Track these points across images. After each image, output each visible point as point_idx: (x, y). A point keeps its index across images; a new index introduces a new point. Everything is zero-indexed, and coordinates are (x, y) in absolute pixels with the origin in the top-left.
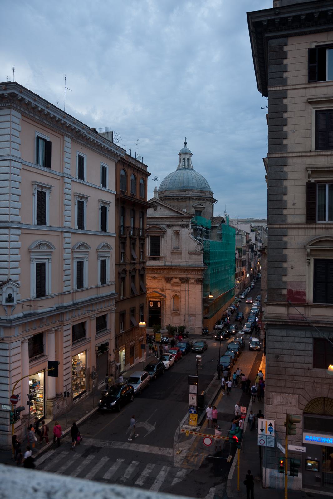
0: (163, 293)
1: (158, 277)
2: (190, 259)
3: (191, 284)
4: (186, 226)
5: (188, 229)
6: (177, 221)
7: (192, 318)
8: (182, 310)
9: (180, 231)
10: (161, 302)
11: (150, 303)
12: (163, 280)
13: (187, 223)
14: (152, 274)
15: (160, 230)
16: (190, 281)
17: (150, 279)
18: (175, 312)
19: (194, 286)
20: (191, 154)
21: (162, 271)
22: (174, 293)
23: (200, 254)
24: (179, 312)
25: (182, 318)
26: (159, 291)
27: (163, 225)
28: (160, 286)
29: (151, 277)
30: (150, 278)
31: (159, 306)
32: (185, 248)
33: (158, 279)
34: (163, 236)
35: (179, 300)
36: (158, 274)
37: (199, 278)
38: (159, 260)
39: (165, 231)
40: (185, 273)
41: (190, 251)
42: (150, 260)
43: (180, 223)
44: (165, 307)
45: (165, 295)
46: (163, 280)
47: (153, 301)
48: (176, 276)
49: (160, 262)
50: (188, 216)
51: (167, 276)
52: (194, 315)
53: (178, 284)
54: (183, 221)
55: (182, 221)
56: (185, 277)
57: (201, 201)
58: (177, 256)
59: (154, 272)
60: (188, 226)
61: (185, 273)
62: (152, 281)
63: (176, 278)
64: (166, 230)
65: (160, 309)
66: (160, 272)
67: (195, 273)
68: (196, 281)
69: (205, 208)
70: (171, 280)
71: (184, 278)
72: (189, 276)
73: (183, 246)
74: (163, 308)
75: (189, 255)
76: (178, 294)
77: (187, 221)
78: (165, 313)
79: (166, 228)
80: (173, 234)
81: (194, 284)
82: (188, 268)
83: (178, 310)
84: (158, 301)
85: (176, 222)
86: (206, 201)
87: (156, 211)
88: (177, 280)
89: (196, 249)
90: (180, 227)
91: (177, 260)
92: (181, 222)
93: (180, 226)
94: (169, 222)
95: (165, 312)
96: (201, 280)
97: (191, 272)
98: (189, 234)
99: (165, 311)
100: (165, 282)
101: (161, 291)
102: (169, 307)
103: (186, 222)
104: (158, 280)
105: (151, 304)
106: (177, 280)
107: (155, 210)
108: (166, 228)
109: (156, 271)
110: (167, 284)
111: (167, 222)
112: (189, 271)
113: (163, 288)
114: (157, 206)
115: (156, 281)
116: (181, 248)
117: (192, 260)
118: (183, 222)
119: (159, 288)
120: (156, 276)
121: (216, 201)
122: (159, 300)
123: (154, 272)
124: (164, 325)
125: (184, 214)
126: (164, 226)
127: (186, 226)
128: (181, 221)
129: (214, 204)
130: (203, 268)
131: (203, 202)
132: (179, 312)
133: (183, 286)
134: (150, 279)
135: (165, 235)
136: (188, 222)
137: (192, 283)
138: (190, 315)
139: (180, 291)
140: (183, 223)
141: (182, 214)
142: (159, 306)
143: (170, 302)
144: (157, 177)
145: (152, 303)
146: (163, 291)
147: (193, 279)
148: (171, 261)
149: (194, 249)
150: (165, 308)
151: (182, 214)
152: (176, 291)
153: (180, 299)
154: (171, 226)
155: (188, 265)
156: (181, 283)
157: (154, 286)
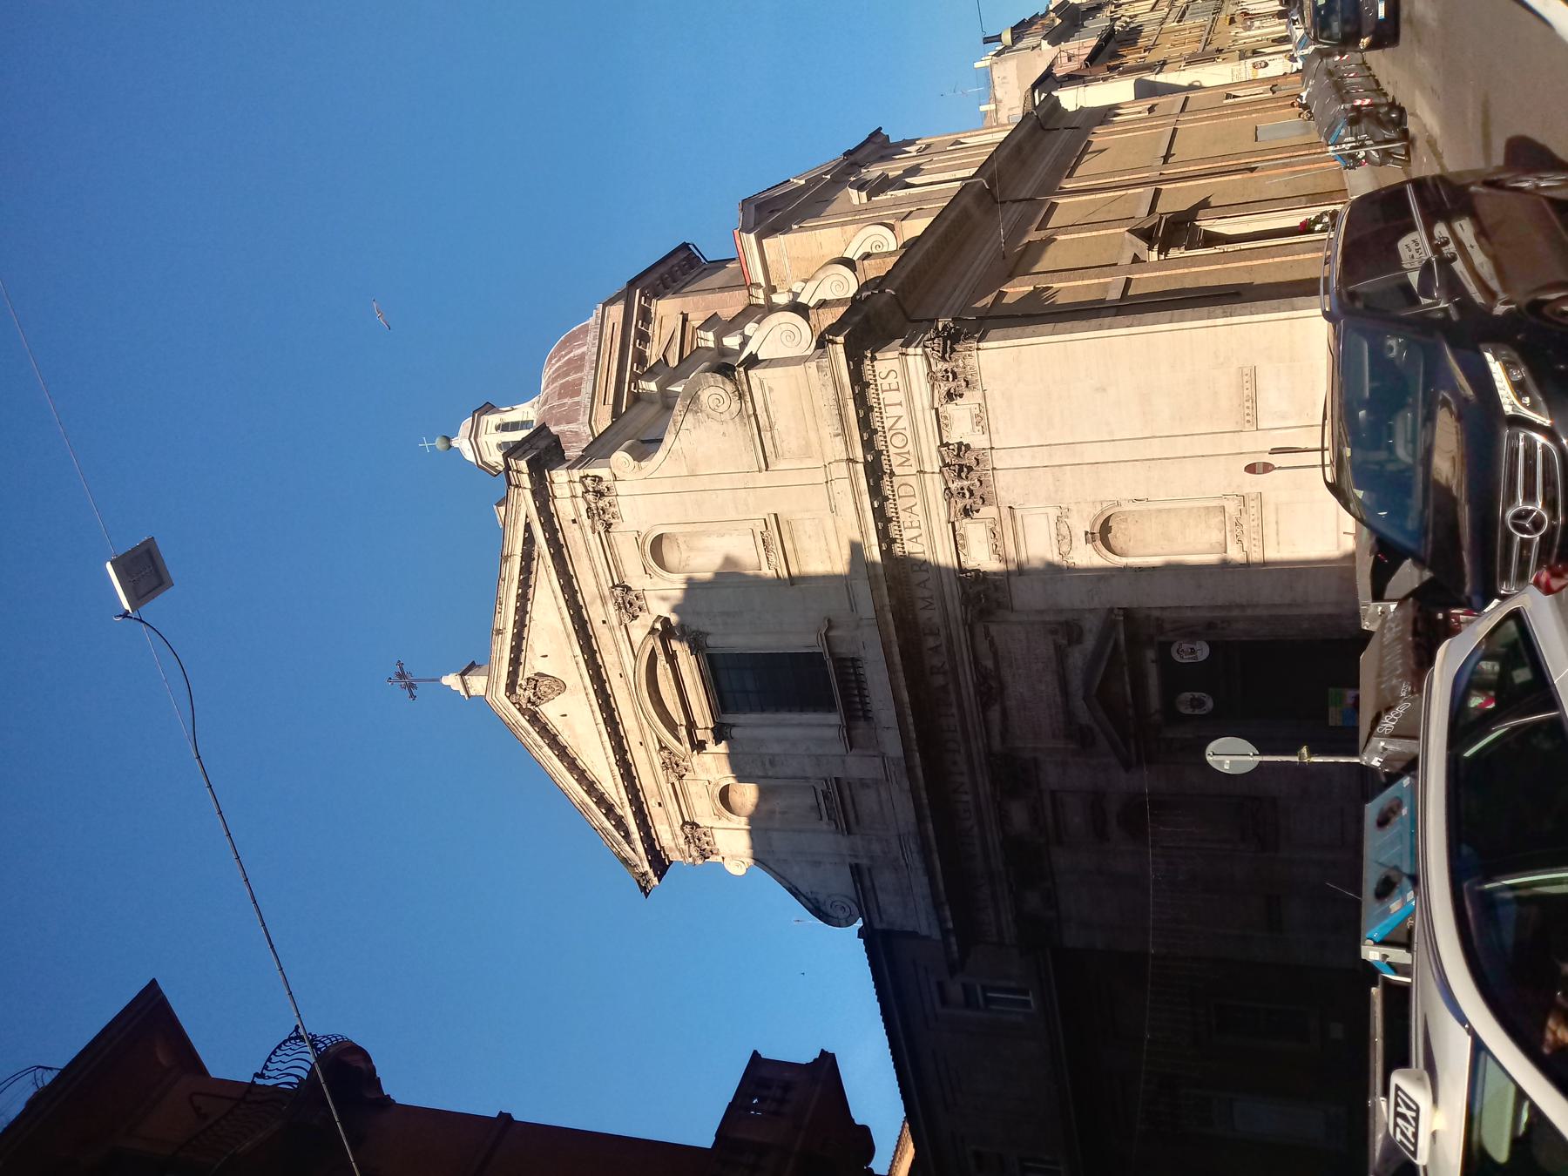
3: (987, 430)
9: (643, 531)
10: (1162, 638)
12: (993, 629)
14: (960, 706)
19: (996, 404)
24: (1232, 507)
29: (985, 707)
33: (989, 664)
43: (594, 541)
50: (528, 494)
52: (1250, 378)
53: (1007, 522)
55: (574, 521)
56: (938, 477)
59: (944, 688)
61: (913, 481)
64: (659, 617)
66: (936, 649)
75: (782, 465)
78: (1249, 612)
82: (860, 467)
90: (616, 535)
92: (581, 528)
95: (1242, 607)
99: (1235, 613)
105: (1199, 703)
107: (559, 686)
109: (939, 680)
110: (1017, 603)
113: (1054, 632)
122: (1151, 654)
126: (639, 631)
127: (599, 494)
128: (576, 526)
132: (1232, 507)
133: (1006, 486)
134: (1004, 713)
137: (981, 420)
140: (587, 522)
141: (528, 527)
142: (1203, 652)
144: (394, 677)
145: (1187, 695)
149: (731, 427)
151: (528, 527)
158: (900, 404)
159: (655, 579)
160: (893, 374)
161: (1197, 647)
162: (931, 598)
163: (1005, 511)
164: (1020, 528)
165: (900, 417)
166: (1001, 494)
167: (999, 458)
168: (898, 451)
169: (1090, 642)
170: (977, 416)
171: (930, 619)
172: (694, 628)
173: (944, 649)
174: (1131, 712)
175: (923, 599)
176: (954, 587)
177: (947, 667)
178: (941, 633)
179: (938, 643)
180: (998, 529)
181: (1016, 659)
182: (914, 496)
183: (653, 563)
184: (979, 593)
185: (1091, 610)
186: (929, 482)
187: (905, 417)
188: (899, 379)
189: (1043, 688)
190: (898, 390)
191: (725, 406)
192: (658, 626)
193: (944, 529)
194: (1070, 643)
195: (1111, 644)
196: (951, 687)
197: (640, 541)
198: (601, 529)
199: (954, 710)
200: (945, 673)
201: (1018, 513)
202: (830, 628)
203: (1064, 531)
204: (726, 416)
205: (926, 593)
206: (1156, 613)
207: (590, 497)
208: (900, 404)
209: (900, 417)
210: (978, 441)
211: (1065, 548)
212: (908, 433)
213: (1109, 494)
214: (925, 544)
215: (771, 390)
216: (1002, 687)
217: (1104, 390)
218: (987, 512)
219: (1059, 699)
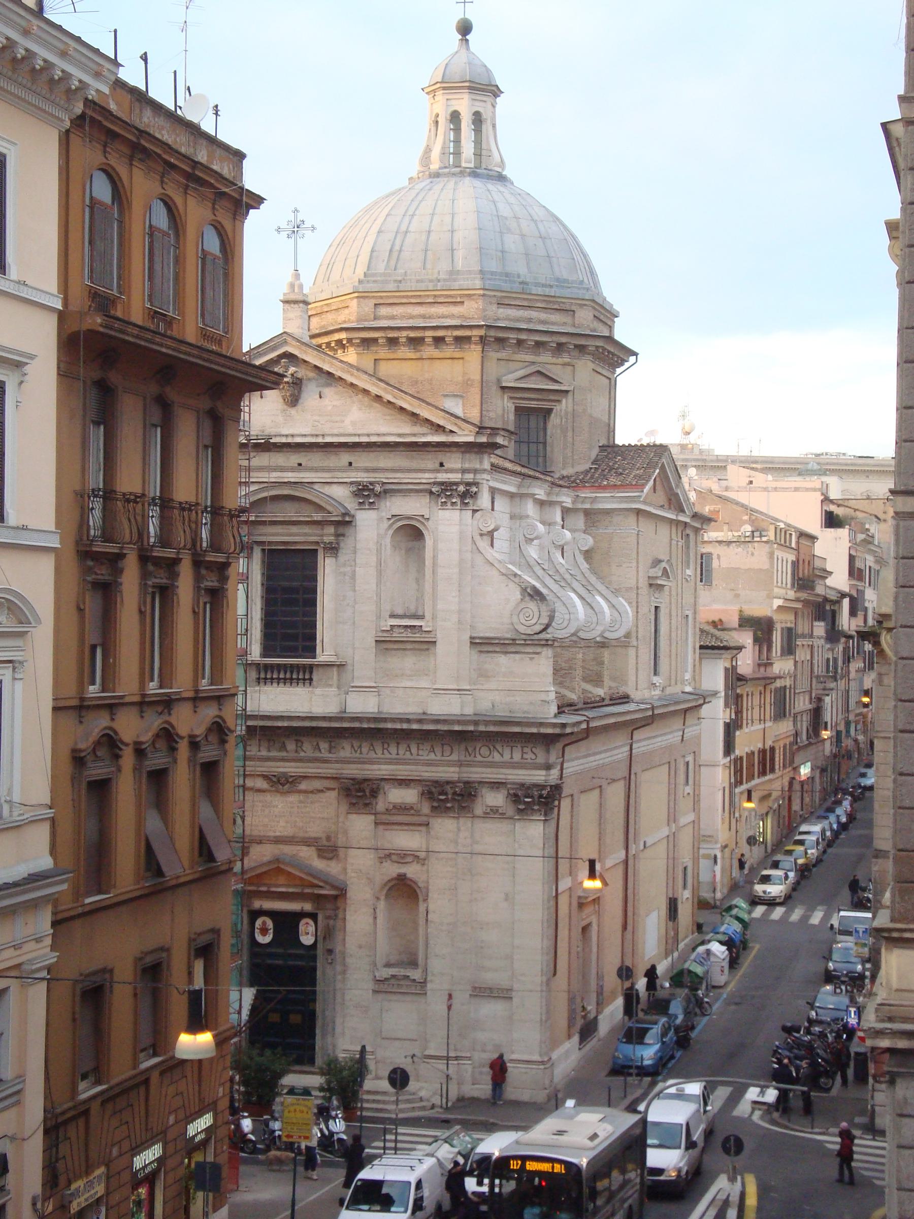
0: (332, 868)
1: (305, 777)
2: (483, 675)
4: (463, 496)
5: (475, 511)
6: (414, 464)
7: (490, 1009)
8: (435, 965)
10: (320, 918)
11: (259, 923)
12: (334, 794)
13: (469, 477)
14: (268, 759)
15: (318, 517)
16: (480, 799)
17: (259, 791)
18: (393, 976)
19: (505, 826)
20: (495, 92)
21: (324, 746)
22: (392, 870)
23: (539, 649)
24: (416, 974)
25: (436, 1004)
26: (307, 854)
27: (334, 487)
28: (315, 830)
29: (265, 777)
30: (261, 783)
31: (307, 940)
32: (455, 618)
33: (303, 786)
34: (333, 549)
35: (422, 907)
36: (301, 760)
37: (536, 785)
38: (311, 679)
39: (345, 523)
40: (454, 757)
41: (485, 630)
42: (258, 680)
44: (338, 948)
45: (341, 877)
46: (334, 794)
47: (271, 914)
48: (403, 771)
49: (318, 691)
50: (471, 439)
51: (353, 771)
52: (504, 994)
54: (447, 465)
55: (442, 465)
56: (455, 777)
57: (546, 358)
58: (408, 661)
60: (474, 496)
62: (268, 797)
63: (404, 783)
64: (353, 516)
65: (314, 958)
67: (507, 757)
68: (515, 798)
69: (570, 394)
70: (374, 793)
71: (448, 783)
72: (476, 774)
73: (440, 606)
74: (330, 951)
75: (475, 655)
76: (412, 871)
77: (467, 466)
79: (351, 505)
80: (388, 540)
81: (503, 816)
83: (414, 964)
84: (302, 915)
85: (409, 471)
86: (576, 353)
87: (293, 411)
88: (409, 796)
89: (515, 619)
90: (426, 499)
91: (409, 684)
92: (438, 471)
93: (431, 493)
94: (367, 470)
96: (541, 796)
97: (485, 751)
98: (477, 538)
100: (344, 807)
101: (320, 856)
102: (360, 947)
103: (464, 471)
104: (305, 792)
105: (264, 931)
106: (409, 796)
107: (293, 401)
108: (351, 505)
110: (353, 817)
111: (358, 469)
112: (478, 745)
113: (328, 838)
114: (297, 383)
115: (293, 798)
116: (434, 618)
117: (493, 685)
118: (447, 471)
119: (307, 842)
120: (291, 769)
121: (632, 359)
122: (308, 907)
123: (283, 748)
124: (334, 1046)
125: (449, 427)
126: (340, 493)
127: (463, 496)
128: (437, 465)
129: (618, 371)
130: (554, 725)
131: (560, 361)
132: (416, 974)
134: (259, 791)
135: (346, 545)
136: (475, 471)
137: (493, 813)
138: (482, 992)
139: (422, 855)
140: (442, 477)
142: (307, 940)
143: (371, 920)
144: (300, 217)
145: (270, 924)
146: (331, 859)
147: (496, 785)
148: (376, 689)
150: (343, 953)
151: (440, 428)
152: (402, 857)
153: (425, 900)
154: (378, 495)
155: (469, 710)
156: (434, 809)
157: (281, 828)
158: (512, 758)
159: (386, 524)
160: (534, 757)
161: (309, 936)
162: (361, 753)
163: (424, 819)
164: (411, 828)
165: (502, 756)
166: (439, 820)
167: (465, 823)
168: (477, 749)
169: (319, 864)
170: (497, 811)
171: (343, 748)
172: (342, 545)
173: (318, 755)
174: (264, 889)
175: (360, 747)
176: (369, 772)
177: (302, 754)
178: (331, 755)
179: (323, 751)
180: (412, 812)
181: (306, 807)
182: (443, 755)
183: (400, 524)
184: (364, 791)
185: (345, 869)
186: (452, 769)
187: (501, 759)
188: (529, 761)
189: (282, 823)
190: (522, 758)
191: (523, 621)
192: (347, 519)
193: (415, 773)
194: (319, 850)
195: (321, 884)
196: (284, 754)
197: (420, 519)
198: (435, 489)
199: (264, 753)
200: (296, 751)
201: (423, 829)
202: (341, 666)
203: (409, 859)
204: (515, 619)
205: (365, 750)
206: (341, 916)
207: (461, 488)
208: (512, 758)
209: (502, 756)
210: (479, 810)
211: (394, 857)
212: (490, 759)
213: (433, 895)
214: (405, 757)
215: (531, 659)
216: (283, 793)
217: (506, 900)
218: (426, 808)
219: (271, 834)
